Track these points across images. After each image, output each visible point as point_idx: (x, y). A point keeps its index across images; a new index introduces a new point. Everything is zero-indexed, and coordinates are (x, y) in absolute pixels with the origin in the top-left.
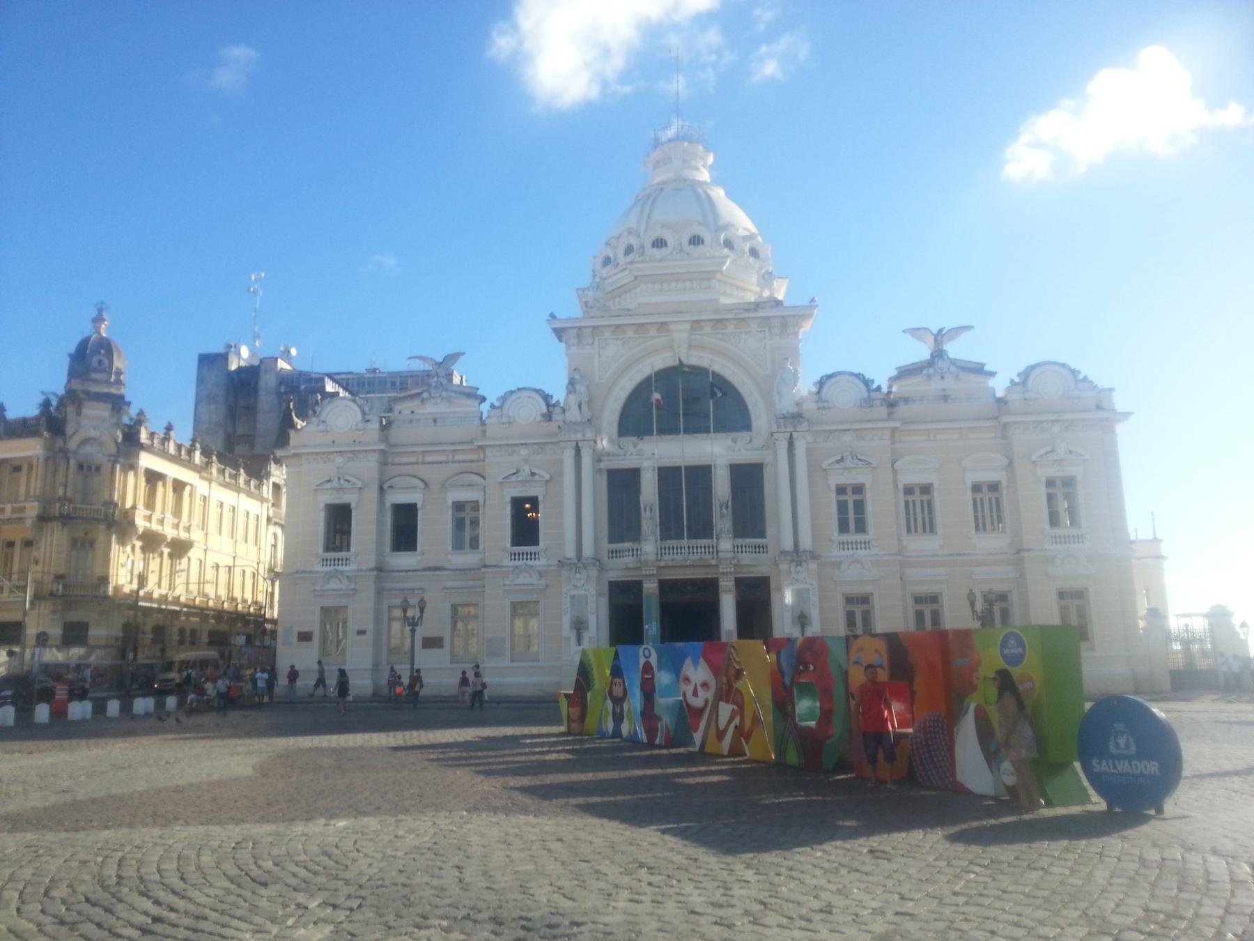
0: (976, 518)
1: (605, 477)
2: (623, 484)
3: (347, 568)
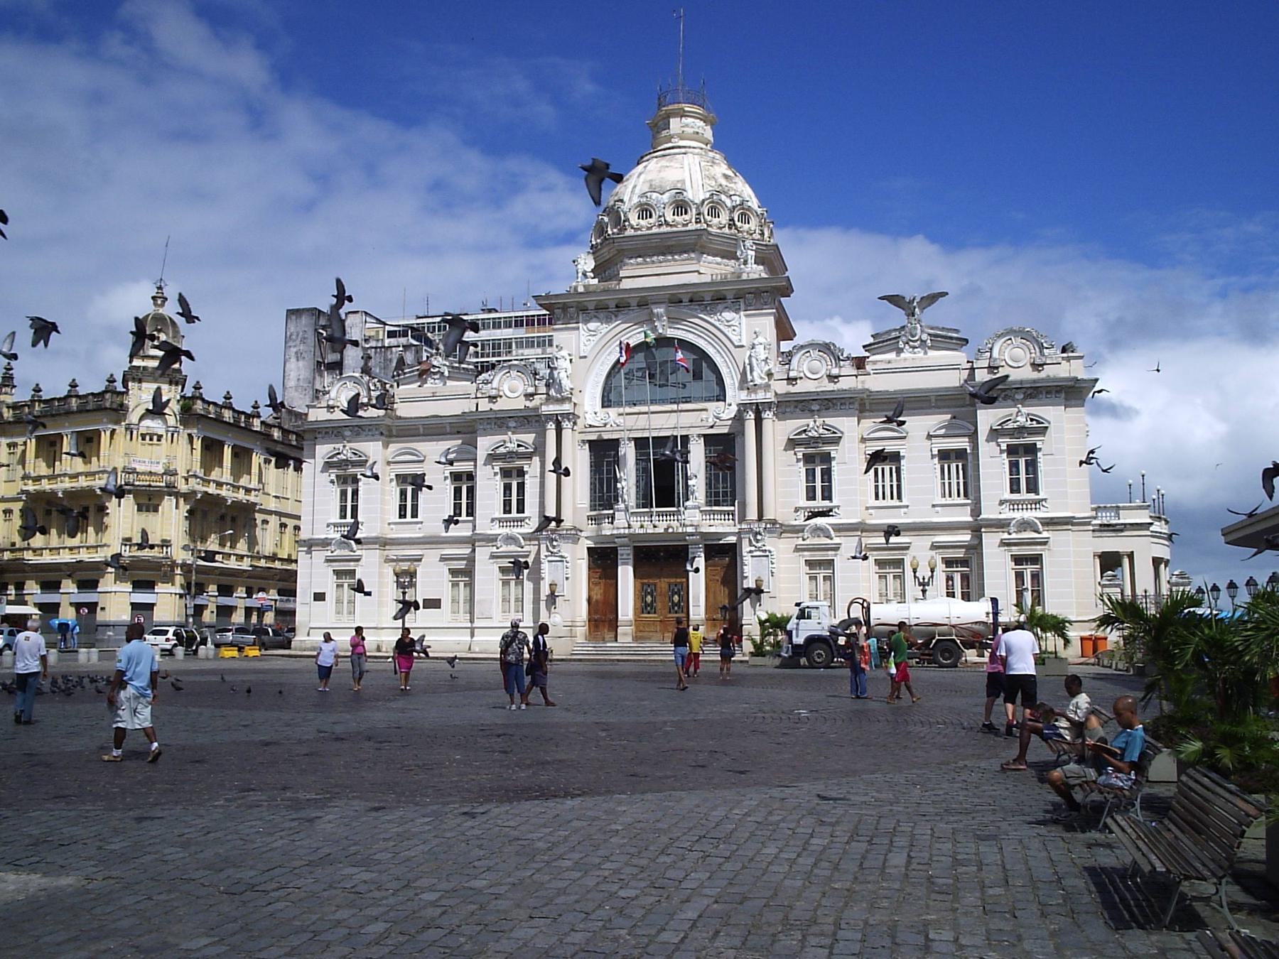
2: (604, 452)
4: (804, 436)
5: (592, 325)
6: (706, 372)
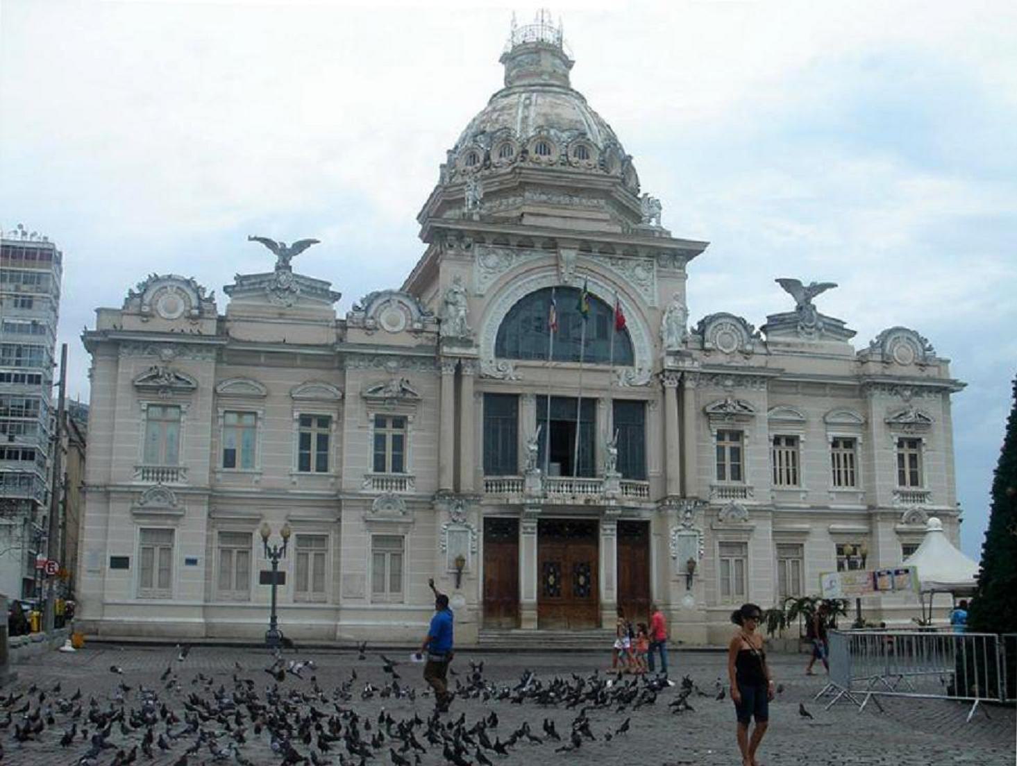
1: (481, 399)
2: (501, 408)
3: (175, 484)
4: (721, 411)
5: (492, 260)
6: (613, 333)
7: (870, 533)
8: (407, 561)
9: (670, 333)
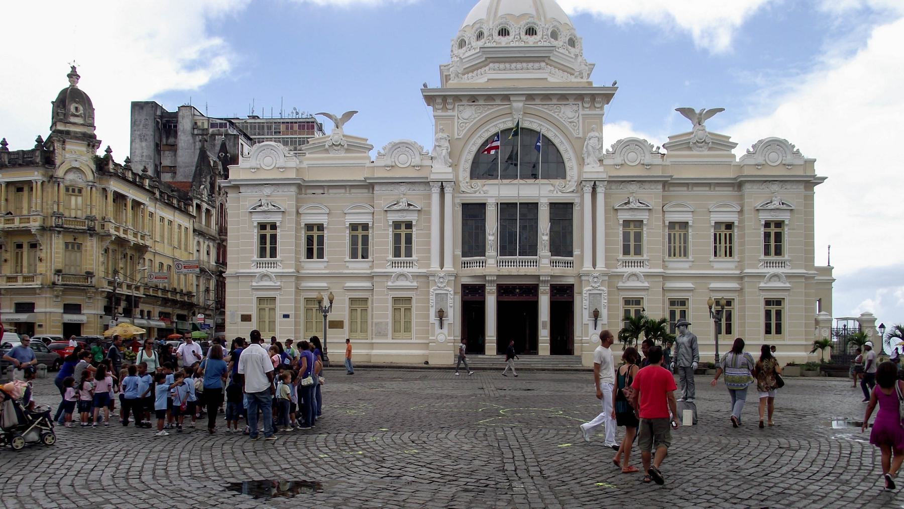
0: (715, 247)
2: (473, 213)
4: (625, 207)
7: (740, 291)
8: (414, 311)
9: (589, 155)
